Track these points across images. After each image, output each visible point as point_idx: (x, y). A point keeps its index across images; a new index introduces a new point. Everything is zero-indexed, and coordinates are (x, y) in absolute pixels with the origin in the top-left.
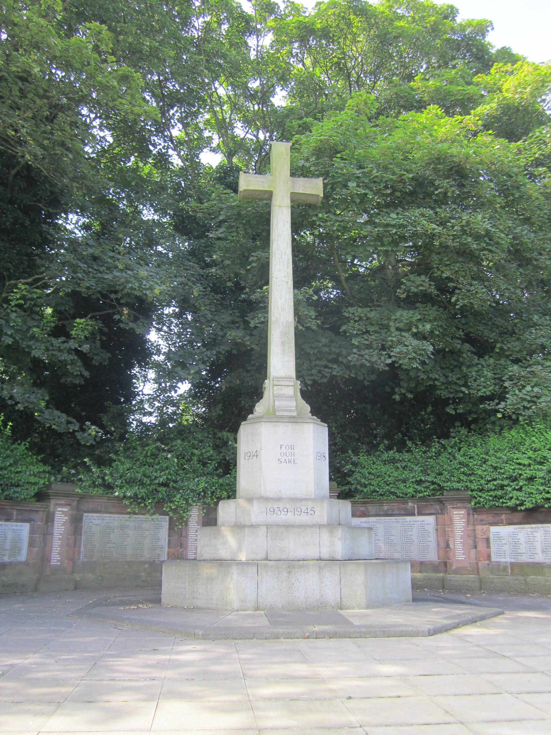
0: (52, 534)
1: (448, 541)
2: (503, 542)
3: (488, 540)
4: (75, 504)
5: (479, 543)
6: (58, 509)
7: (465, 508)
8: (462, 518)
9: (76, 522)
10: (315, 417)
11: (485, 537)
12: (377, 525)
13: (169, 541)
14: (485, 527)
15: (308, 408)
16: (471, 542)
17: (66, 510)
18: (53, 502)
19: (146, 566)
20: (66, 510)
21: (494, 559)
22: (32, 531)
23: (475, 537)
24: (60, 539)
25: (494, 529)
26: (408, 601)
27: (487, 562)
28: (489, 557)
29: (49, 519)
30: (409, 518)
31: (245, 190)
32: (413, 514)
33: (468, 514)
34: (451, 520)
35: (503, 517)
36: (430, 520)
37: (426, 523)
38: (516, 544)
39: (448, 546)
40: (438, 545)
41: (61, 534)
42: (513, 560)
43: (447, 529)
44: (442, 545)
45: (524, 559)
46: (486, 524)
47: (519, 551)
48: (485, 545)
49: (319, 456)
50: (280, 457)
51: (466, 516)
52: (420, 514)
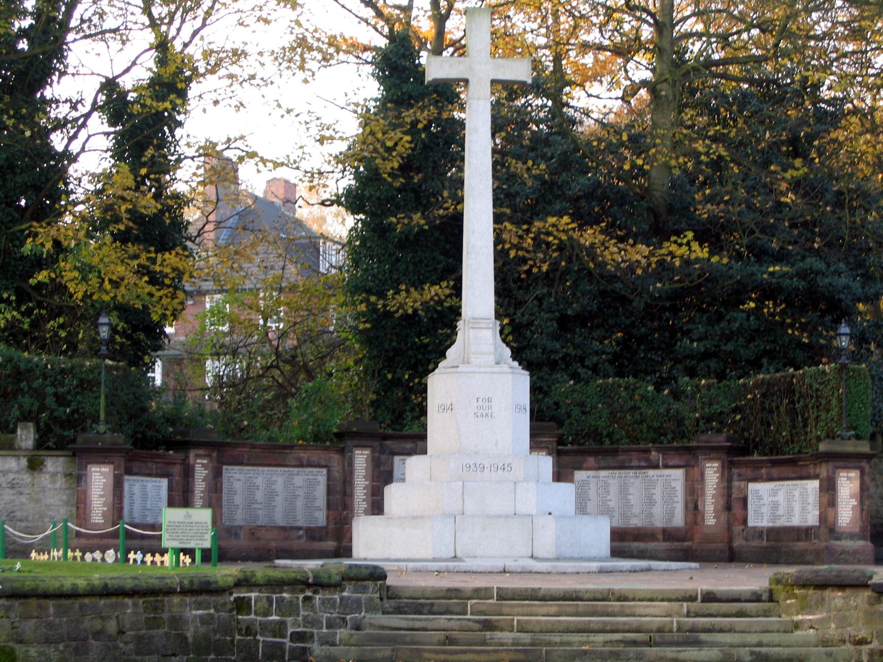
0: (193, 492)
1: (697, 501)
2: (762, 502)
3: (745, 501)
4: (215, 454)
5: (734, 504)
6: (198, 461)
7: (720, 459)
8: (715, 472)
9: (217, 474)
10: (516, 364)
11: (741, 496)
12: (610, 481)
13: (328, 500)
14: (743, 484)
15: (508, 352)
16: (722, 502)
17: (205, 462)
18: (192, 454)
19: (301, 532)
20: (205, 462)
21: (751, 523)
22: (170, 488)
23: (729, 496)
24: (201, 498)
25: (752, 486)
26: (607, 557)
27: (743, 527)
28: (745, 521)
29: (188, 473)
30: (651, 472)
31: (434, 80)
32: (656, 467)
33: (723, 467)
34: (702, 474)
35: (763, 471)
36: (679, 473)
37: (672, 478)
38: (775, 506)
39: (696, 507)
40: (686, 507)
41: (202, 492)
42: (771, 525)
43: (696, 486)
44: (691, 506)
45: (781, 523)
46: (744, 480)
47: (777, 513)
48: (741, 505)
49: (519, 408)
50: (476, 411)
51: (720, 470)
52: (666, 466)
